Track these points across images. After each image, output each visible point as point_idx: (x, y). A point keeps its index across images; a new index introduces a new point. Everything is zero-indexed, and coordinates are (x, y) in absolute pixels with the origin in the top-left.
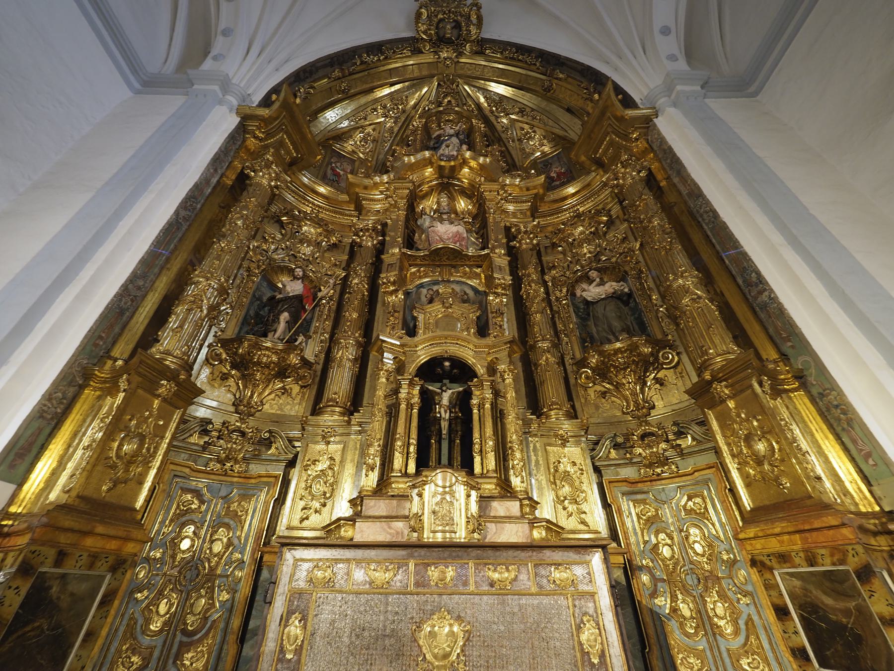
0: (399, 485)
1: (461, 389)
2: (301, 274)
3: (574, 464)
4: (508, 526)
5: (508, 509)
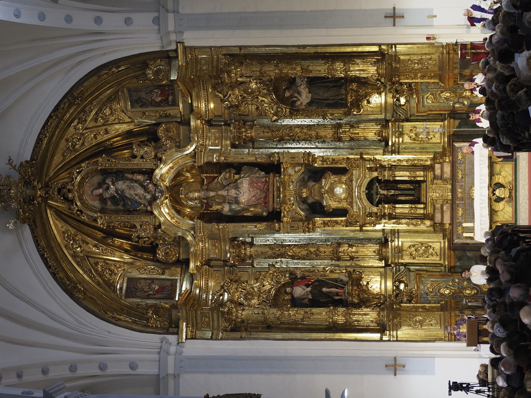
0: (430, 210)
1: (377, 184)
2: (289, 289)
3: (411, 130)
4: (445, 170)
5: (438, 168)
